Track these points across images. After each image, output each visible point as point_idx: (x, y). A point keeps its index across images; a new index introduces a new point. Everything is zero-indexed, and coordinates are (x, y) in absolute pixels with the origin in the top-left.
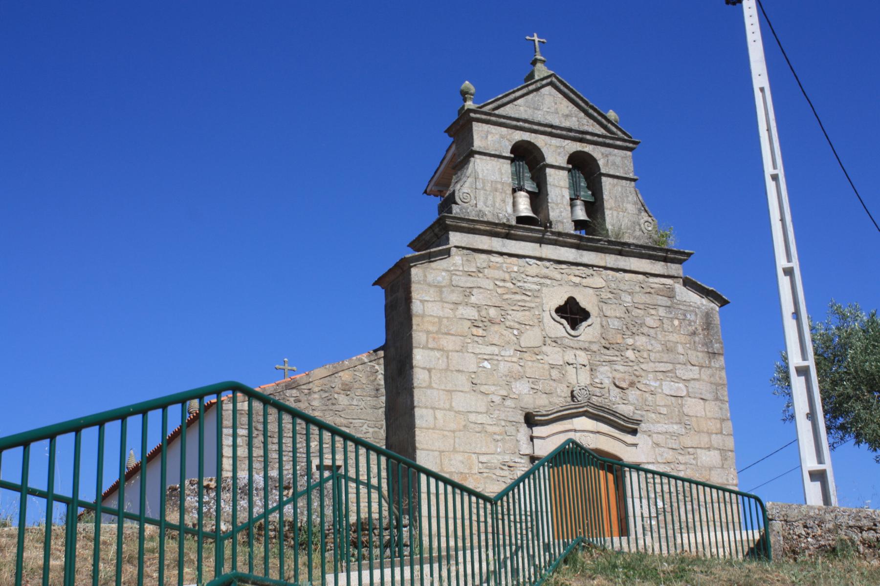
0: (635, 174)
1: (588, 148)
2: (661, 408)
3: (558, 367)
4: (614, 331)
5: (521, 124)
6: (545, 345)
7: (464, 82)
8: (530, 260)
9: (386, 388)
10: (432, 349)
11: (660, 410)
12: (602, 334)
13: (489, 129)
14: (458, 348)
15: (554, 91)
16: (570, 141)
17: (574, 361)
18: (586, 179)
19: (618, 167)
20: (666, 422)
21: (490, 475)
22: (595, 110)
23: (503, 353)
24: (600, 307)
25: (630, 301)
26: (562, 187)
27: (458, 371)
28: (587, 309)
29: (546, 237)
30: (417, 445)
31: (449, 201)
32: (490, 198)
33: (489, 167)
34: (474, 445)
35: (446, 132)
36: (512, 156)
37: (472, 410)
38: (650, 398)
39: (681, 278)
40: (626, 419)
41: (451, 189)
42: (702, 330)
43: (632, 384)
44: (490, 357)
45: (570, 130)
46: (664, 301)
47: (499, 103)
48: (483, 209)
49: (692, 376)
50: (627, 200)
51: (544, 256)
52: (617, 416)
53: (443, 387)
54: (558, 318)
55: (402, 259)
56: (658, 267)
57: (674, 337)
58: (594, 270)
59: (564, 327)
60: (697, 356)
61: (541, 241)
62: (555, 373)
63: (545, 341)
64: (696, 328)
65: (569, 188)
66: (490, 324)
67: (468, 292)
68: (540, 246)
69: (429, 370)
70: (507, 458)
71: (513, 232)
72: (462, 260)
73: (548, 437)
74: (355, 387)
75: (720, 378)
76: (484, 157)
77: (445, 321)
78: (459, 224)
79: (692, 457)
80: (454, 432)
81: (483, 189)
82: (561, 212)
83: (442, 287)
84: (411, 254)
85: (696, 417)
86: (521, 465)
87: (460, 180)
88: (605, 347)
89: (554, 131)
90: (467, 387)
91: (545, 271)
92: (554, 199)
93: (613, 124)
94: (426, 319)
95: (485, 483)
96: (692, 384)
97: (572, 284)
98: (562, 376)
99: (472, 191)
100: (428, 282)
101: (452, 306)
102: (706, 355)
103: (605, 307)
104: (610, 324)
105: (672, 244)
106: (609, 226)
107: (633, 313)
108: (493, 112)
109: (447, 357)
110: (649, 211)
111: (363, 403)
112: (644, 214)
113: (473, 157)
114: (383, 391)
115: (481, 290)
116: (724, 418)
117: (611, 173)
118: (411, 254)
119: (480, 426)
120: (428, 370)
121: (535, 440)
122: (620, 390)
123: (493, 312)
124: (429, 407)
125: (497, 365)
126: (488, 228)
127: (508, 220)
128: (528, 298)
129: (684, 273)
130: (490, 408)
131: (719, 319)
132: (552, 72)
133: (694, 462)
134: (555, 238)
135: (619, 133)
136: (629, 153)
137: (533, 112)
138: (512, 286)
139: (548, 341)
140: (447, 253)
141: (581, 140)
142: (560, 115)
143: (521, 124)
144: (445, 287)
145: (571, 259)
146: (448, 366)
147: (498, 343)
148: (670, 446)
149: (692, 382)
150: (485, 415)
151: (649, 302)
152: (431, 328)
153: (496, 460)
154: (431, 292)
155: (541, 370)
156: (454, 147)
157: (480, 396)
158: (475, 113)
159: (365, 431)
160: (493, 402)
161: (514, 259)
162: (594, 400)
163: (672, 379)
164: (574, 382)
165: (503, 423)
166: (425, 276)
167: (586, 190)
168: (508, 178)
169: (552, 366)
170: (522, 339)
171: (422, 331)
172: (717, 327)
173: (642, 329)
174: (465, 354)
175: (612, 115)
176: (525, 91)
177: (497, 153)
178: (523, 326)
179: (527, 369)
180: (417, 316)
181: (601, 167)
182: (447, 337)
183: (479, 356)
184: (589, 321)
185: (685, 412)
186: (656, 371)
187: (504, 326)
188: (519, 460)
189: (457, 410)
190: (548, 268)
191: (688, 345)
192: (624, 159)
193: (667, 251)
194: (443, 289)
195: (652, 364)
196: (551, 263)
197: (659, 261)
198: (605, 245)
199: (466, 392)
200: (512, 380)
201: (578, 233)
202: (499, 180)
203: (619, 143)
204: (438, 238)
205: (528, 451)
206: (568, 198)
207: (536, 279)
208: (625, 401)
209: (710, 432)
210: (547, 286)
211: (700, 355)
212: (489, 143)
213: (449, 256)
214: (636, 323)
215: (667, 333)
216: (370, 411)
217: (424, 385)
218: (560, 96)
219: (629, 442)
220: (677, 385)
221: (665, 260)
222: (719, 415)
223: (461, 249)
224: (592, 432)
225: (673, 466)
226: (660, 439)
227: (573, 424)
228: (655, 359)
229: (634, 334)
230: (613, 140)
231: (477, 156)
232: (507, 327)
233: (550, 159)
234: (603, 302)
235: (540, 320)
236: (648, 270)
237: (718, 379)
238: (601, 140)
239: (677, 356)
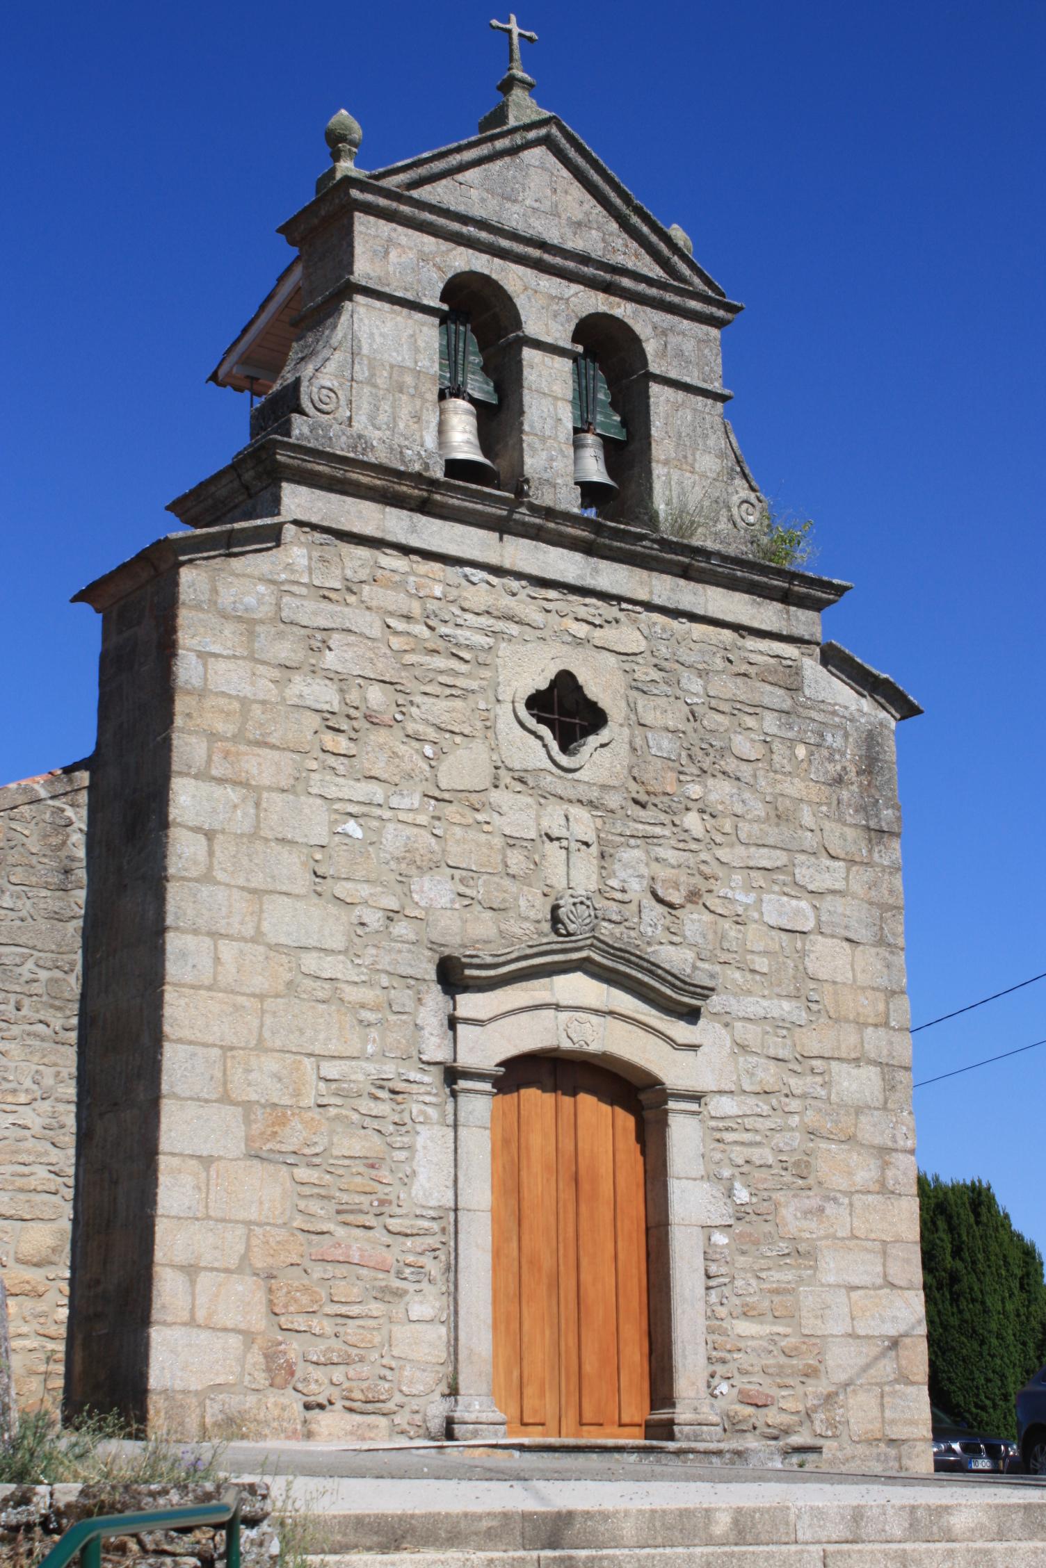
0: (725, 385)
1: (622, 310)
2: (757, 958)
3: (525, 844)
4: (659, 761)
5: (470, 230)
6: (496, 787)
7: (336, 111)
8: (474, 571)
9: (90, 868)
10: (221, 781)
11: (753, 962)
12: (631, 768)
13: (394, 235)
14: (284, 784)
15: (552, 160)
16: (582, 287)
17: (563, 833)
18: (611, 384)
19: (689, 362)
20: (766, 993)
21: (344, 1112)
22: (646, 218)
23: (394, 802)
24: (631, 700)
25: (699, 689)
26: (556, 398)
27: (282, 841)
28: (601, 705)
29: (516, 516)
30: (167, 1029)
31: (289, 401)
32: (386, 406)
33: (387, 328)
34: (309, 1033)
35: (281, 230)
36: (445, 307)
37: (312, 942)
38: (733, 932)
39: (818, 644)
40: (678, 983)
41: (288, 377)
42: (858, 773)
43: (694, 896)
44: (364, 809)
45: (585, 259)
46: (777, 697)
47: (422, 171)
48: (366, 433)
49: (829, 884)
50: (705, 444)
51: (507, 565)
52: (659, 976)
53: (241, 882)
54: (531, 722)
55: (159, 541)
56: (768, 615)
57: (795, 787)
58: (621, 610)
59: (545, 746)
60: (843, 837)
61: (503, 527)
62: (516, 860)
63: (496, 778)
64: (844, 768)
65: (573, 403)
66: (368, 725)
67: (319, 639)
68: (501, 539)
69: (210, 835)
70: (389, 1070)
71: (438, 497)
72: (310, 558)
73: (491, 1020)
74: (11, 860)
75: (891, 892)
76: (378, 304)
77: (257, 710)
78: (309, 466)
79: (819, 1079)
80: (261, 997)
81: (371, 382)
82: (552, 459)
83: (254, 622)
84: (180, 532)
85: (834, 983)
86: (423, 1089)
87: (313, 353)
88: (636, 802)
89: (547, 257)
90: (303, 883)
91: (507, 602)
92: (538, 426)
93: (684, 257)
94: (210, 702)
95: (332, 1132)
96: (828, 903)
97: (570, 639)
98: (532, 867)
99: (341, 385)
100: (220, 606)
101: (276, 673)
102: (861, 833)
103: (641, 701)
104: (651, 743)
105: (803, 560)
106: (660, 505)
107: (705, 723)
108: (406, 193)
109: (257, 805)
110: (751, 476)
111: (29, 903)
112: (739, 482)
113: (351, 300)
114: (82, 874)
115: (352, 638)
116: (895, 987)
117: (673, 374)
118: (180, 532)
119: (327, 985)
120: (205, 835)
121: (460, 1027)
122: (664, 910)
123: (376, 696)
124: (204, 929)
125: (378, 831)
126: (378, 482)
127: (427, 466)
128: (463, 668)
129: (824, 633)
130: (357, 940)
131: (894, 749)
132: (547, 114)
133: (823, 1093)
134: (538, 521)
135: (696, 280)
136: (715, 333)
137: (501, 205)
138: (426, 633)
139: (506, 778)
140: (273, 536)
141: (608, 288)
142: (564, 222)
143: (470, 230)
144: (262, 622)
145: (570, 577)
146: (257, 827)
147: (384, 776)
148: (772, 1053)
149: (829, 898)
150: (341, 957)
151: (742, 698)
152: (220, 727)
153: (360, 1074)
154: (226, 632)
155: (485, 850)
156: (298, 272)
157: (333, 909)
158: (362, 191)
159: (28, 976)
160: (363, 924)
161: (437, 566)
162: (606, 930)
163: (786, 889)
164: (559, 882)
165: (385, 981)
166: (214, 591)
167: (610, 410)
168: (431, 360)
169: (511, 842)
170: (443, 768)
171: (197, 732)
172: (890, 769)
173: (722, 763)
174: (303, 798)
175: (678, 233)
176: (484, 150)
177: (410, 296)
178: (448, 735)
179: (453, 848)
180: (189, 693)
181: (649, 357)
182: (257, 750)
183: (336, 806)
184: (604, 735)
185: (810, 971)
187: (401, 734)
189: (273, 941)
190: (514, 595)
191: (824, 808)
192: (702, 346)
193: (792, 576)
194: (259, 629)
195: (741, 850)
196: (524, 583)
197: (772, 599)
198: (652, 549)
199: (297, 896)
200: (413, 871)
201: (591, 513)
202: (410, 364)
203: (694, 304)
204: (250, 496)
205: (443, 1055)
206: (570, 426)
207: (484, 621)
208: (675, 936)
209: (861, 1020)
210: (511, 639)
211: (850, 833)
212: (391, 269)
213: (278, 546)
214: (712, 745)
215: (779, 777)
216: (44, 925)
217: (194, 873)
218: (565, 173)
219: (680, 1041)
220: (794, 902)
221: (786, 598)
222: (883, 982)
223: (307, 529)
224: (596, 1012)
225: (774, 1102)
226: (750, 1033)
227: (552, 990)
228: (749, 836)
229: (705, 772)
230: (682, 296)
231: (359, 298)
232: (408, 736)
233: (533, 325)
234: (637, 689)
235: (488, 724)
236: (746, 621)
237: (886, 893)
238: (653, 292)
239: (800, 832)
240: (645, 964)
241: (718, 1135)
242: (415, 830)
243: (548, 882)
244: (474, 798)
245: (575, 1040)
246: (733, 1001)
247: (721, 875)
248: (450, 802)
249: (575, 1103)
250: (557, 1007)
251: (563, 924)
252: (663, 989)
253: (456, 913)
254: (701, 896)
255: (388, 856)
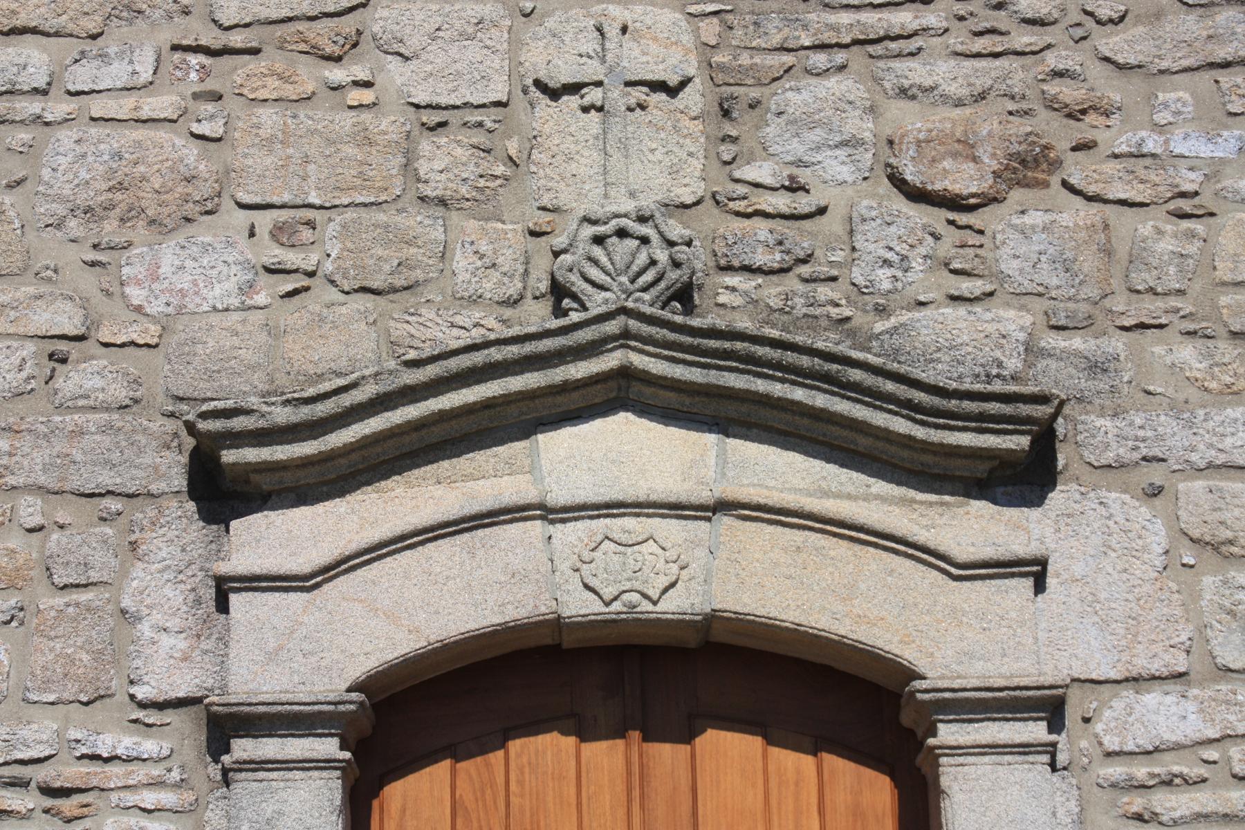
17: (593, 70)
23: (81, 77)
86: (140, 773)
98: (500, 169)
122: (937, 217)
125: (28, 152)
147: (51, 24)
155: (350, 150)
165: (30, 510)
186: (1226, 65)
188: (125, 743)
200: (140, 231)
219: (963, 553)
224: (676, 509)
227: (533, 469)
240: (805, 361)
241: (1137, 803)
242: (140, 133)
243: (546, 201)
244: (322, 33)
245: (608, 593)
246: (1166, 423)
247: (1117, 97)
248: (255, 52)
249: (693, 756)
250: (549, 513)
251: (574, 297)
252: (879, 419)
253: (258, 316)
254: (1056, 164)
255: (61, 210)
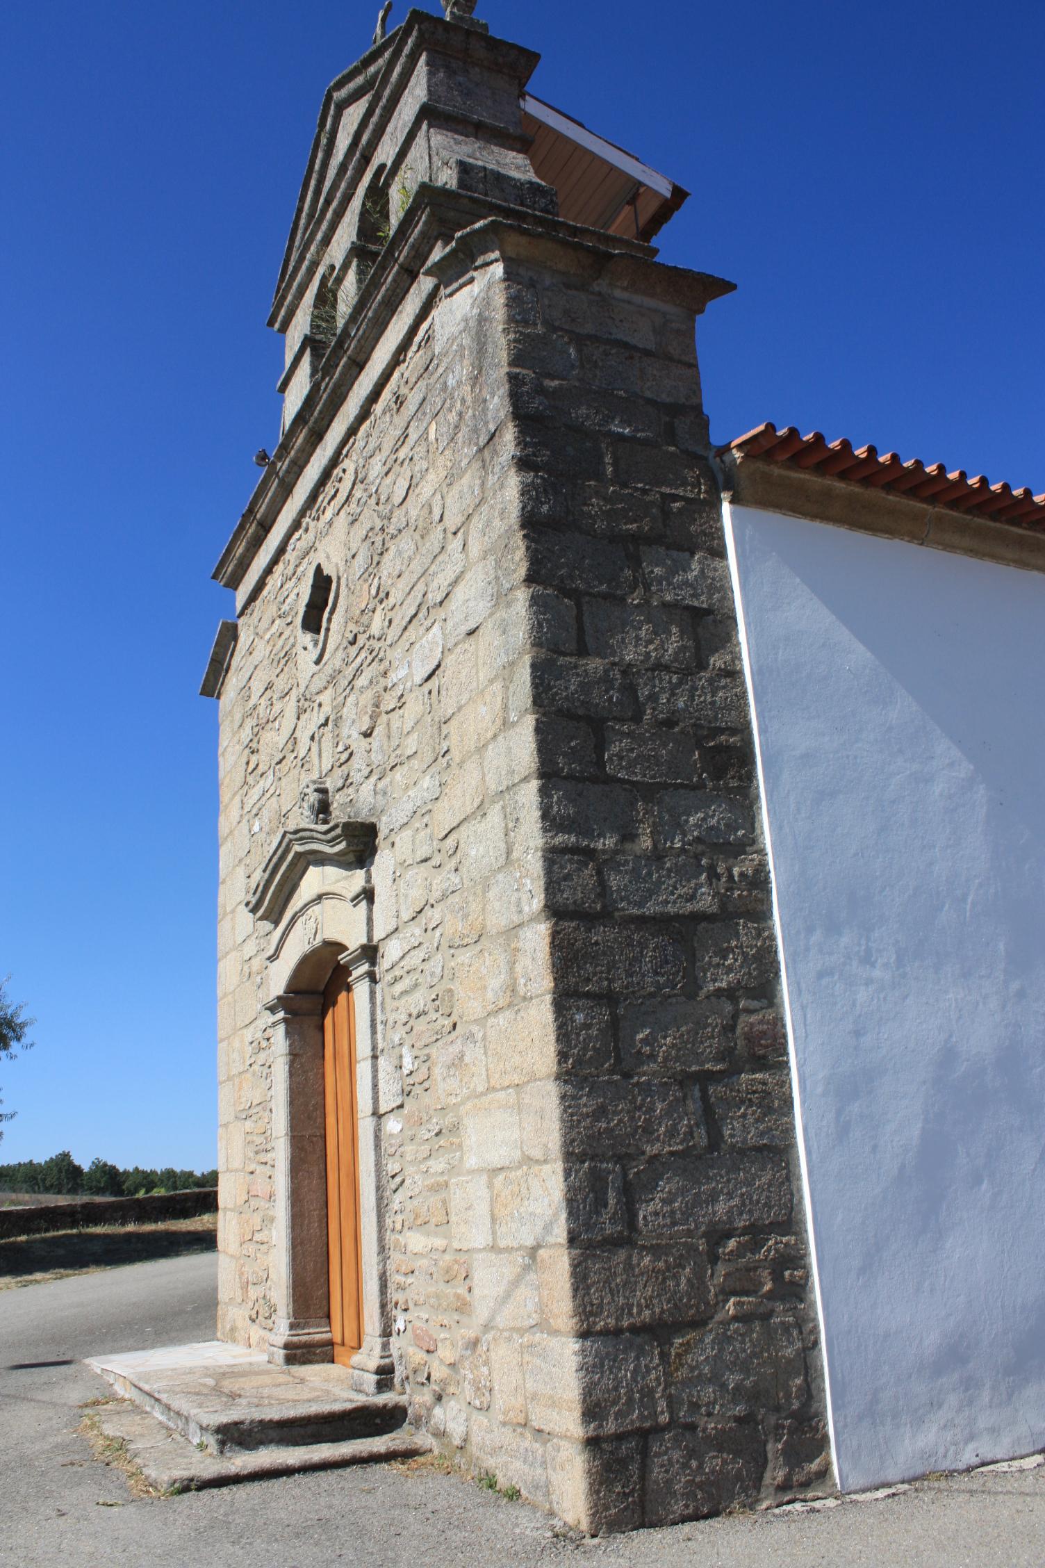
29: (281, 474)
198: (328, 384)
